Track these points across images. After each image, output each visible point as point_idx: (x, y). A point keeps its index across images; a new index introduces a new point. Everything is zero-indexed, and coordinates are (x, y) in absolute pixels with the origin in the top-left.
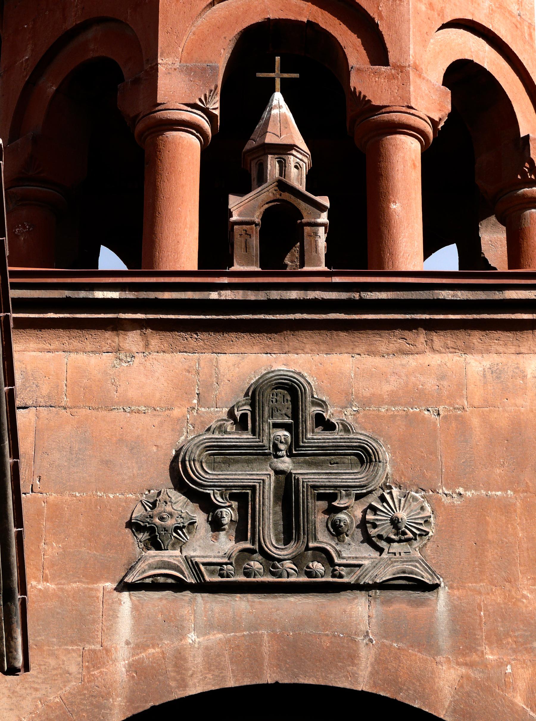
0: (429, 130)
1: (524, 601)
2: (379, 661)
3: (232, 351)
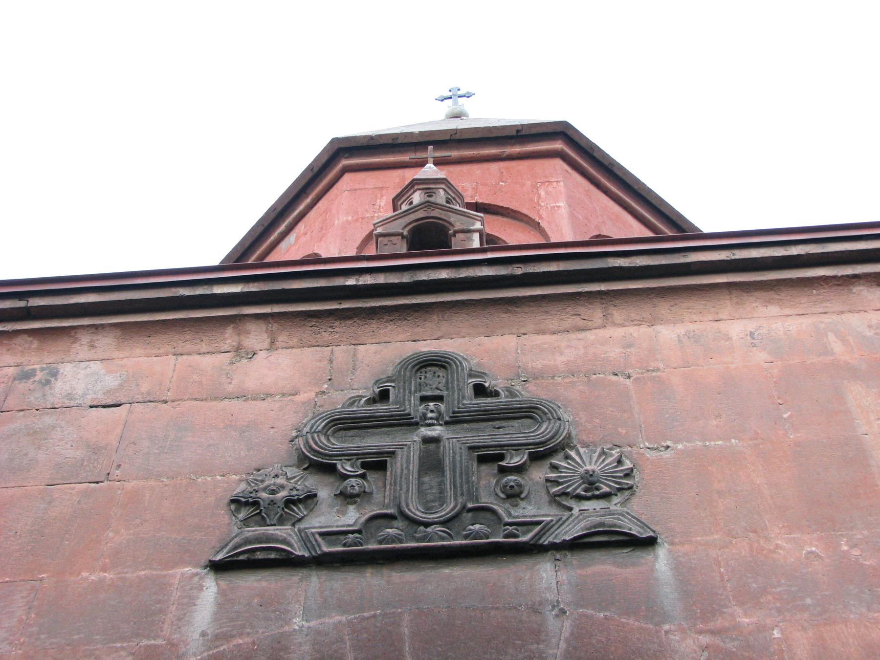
1: (781, 552)
2: (579, 635)
3: (373, 341)
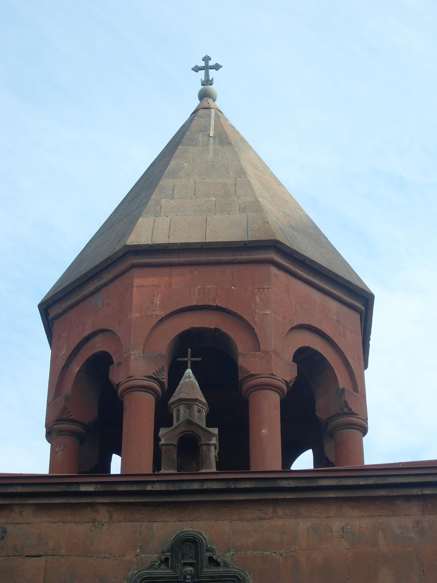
0: (285, 387)
